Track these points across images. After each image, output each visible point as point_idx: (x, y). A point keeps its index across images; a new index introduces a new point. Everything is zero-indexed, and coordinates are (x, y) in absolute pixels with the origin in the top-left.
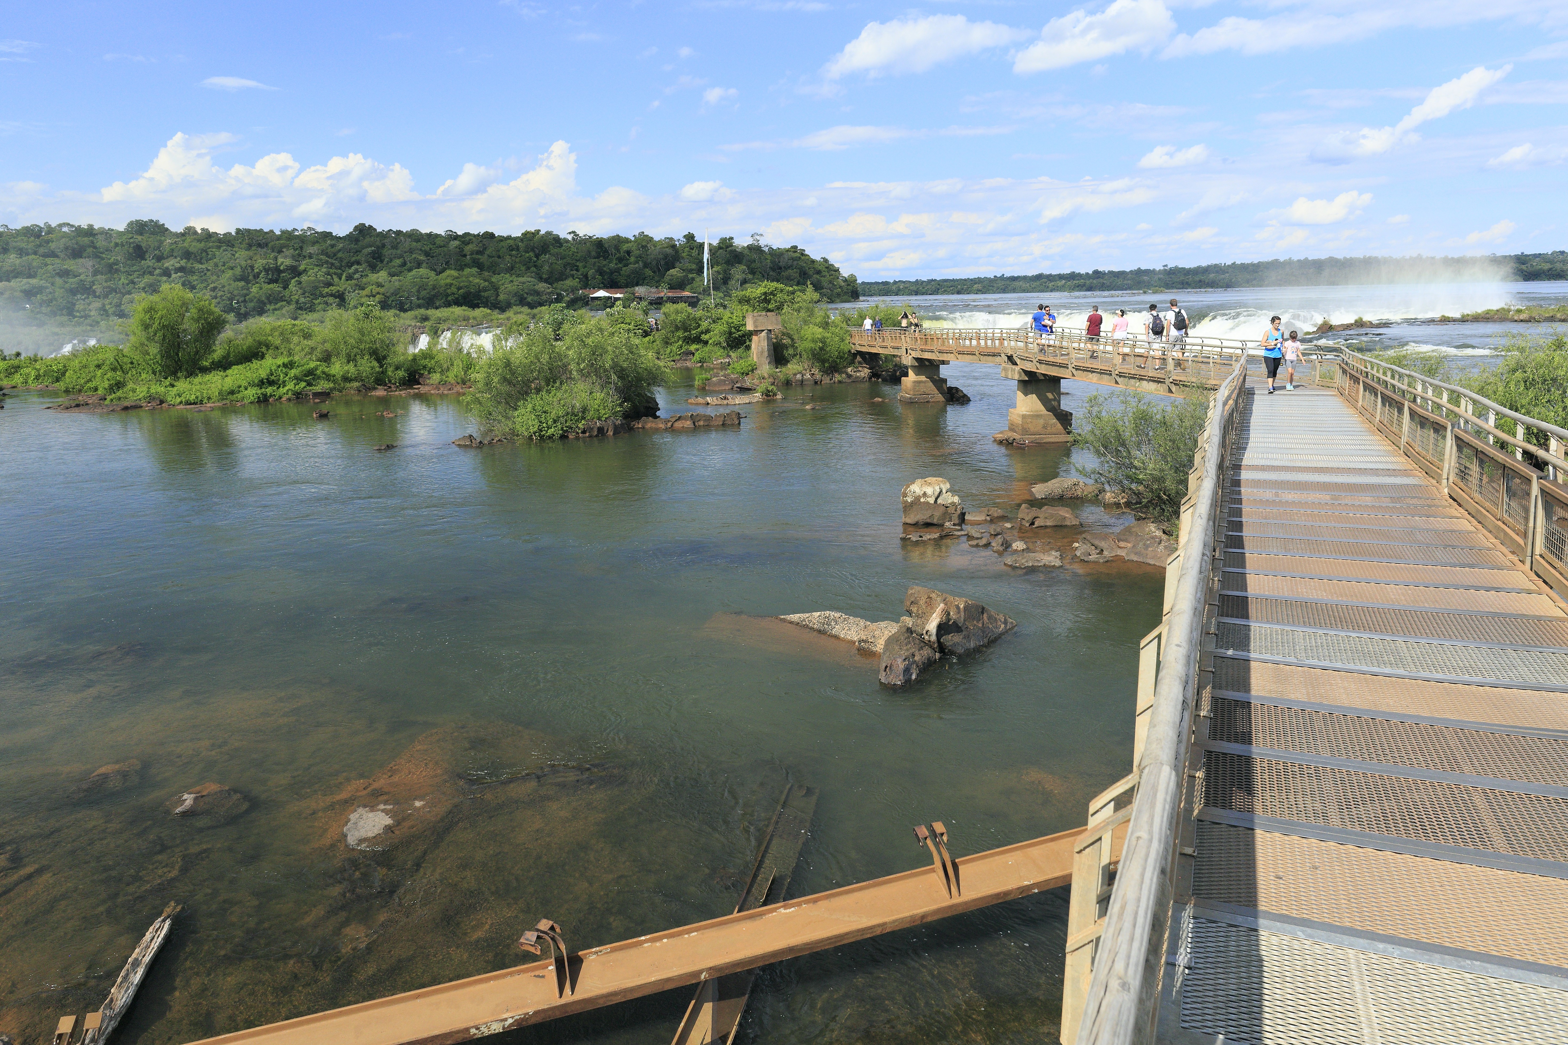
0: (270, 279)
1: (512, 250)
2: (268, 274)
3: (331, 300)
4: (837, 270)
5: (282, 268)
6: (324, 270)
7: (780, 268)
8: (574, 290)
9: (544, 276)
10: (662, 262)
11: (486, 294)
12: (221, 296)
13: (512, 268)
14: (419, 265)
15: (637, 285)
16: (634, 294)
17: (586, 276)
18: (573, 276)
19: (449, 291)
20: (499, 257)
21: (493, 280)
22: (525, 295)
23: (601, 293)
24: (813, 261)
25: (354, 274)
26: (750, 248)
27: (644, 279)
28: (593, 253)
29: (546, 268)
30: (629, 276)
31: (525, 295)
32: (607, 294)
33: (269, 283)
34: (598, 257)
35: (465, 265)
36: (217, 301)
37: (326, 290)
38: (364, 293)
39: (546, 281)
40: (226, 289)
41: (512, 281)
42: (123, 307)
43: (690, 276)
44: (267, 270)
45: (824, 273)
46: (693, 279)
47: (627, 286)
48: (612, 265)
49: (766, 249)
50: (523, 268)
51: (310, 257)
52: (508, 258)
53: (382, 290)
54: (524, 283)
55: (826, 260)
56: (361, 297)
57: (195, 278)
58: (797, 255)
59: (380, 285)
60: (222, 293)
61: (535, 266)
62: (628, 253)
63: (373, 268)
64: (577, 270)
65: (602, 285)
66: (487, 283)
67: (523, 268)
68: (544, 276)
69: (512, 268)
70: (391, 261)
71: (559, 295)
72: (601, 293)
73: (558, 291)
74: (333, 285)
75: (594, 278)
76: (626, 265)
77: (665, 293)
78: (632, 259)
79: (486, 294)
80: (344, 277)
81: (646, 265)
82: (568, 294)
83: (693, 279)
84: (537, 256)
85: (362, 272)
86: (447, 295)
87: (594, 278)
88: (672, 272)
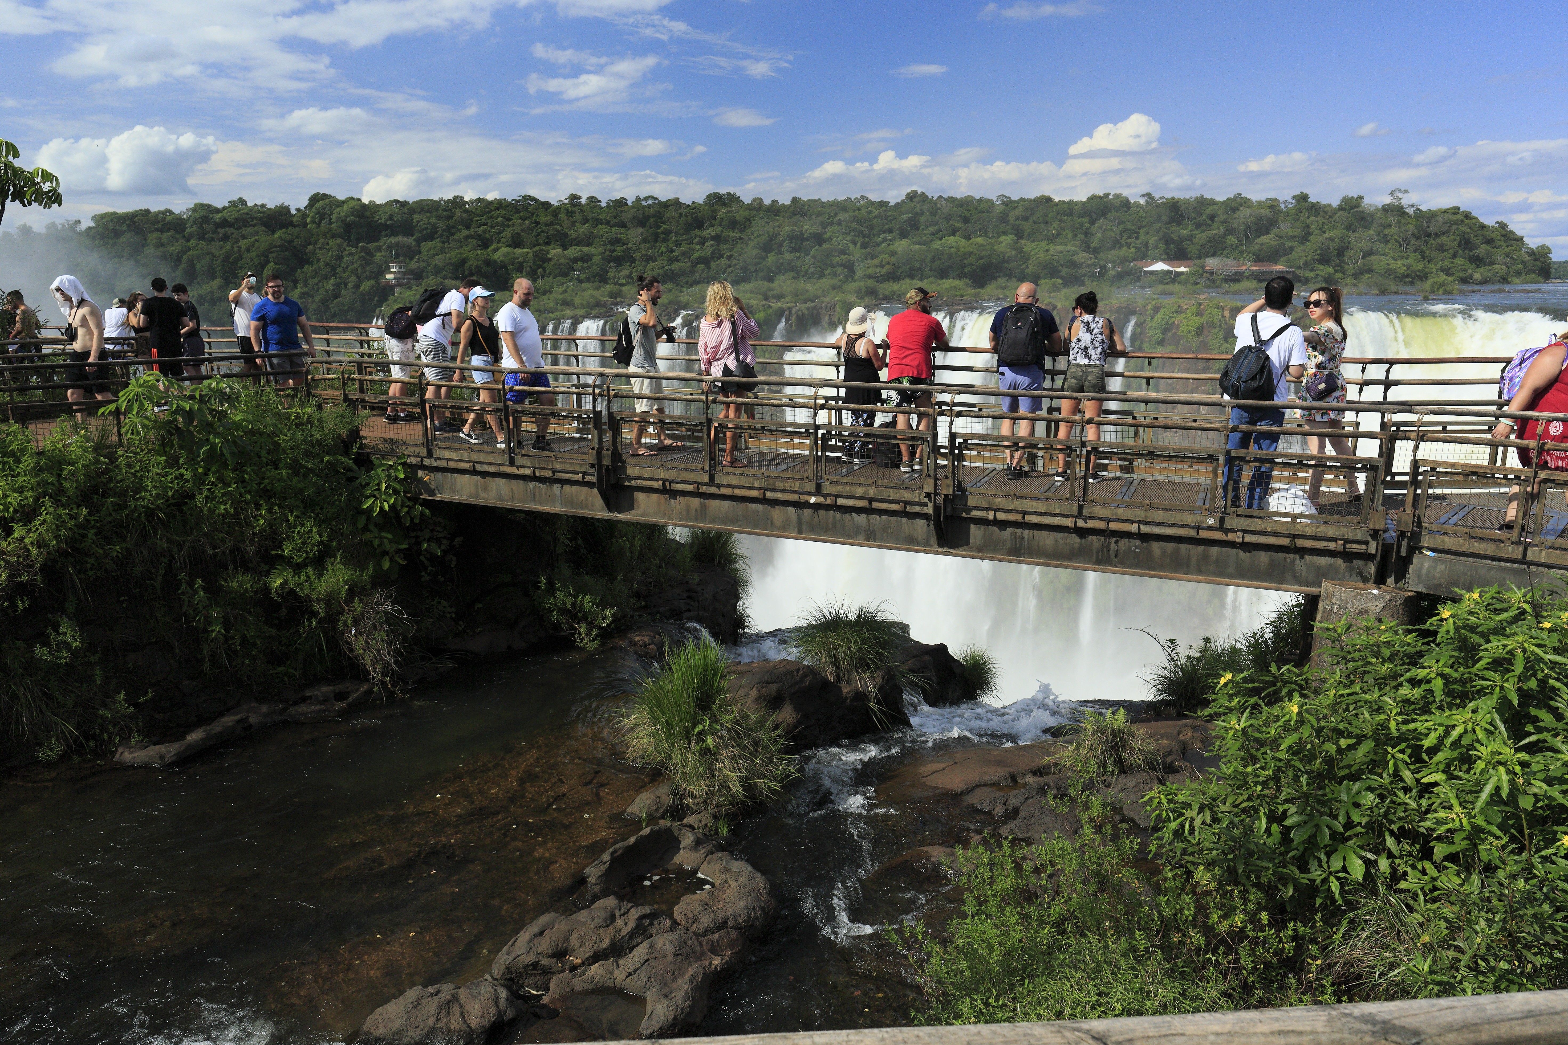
4: (1520, 239)
7: (1429, 235)
10: (1253, 227)
17: (1146, 246)
24: (1483, 227)
26: (1387, 209)
28: (1165, 218)
30: (1203, 245)
43: (1289, 244)
44: (791, 238)
45: (1498, 243)
46: (1292, 249)
49: (1411, 211)
51: (840, 223)
52: (1056, 224)
55: (1503, 226)
58: (1460, 217)
81: (1230, 231)
83: (1292, 249)
84: (1093, 222)
88: (1264, 239)
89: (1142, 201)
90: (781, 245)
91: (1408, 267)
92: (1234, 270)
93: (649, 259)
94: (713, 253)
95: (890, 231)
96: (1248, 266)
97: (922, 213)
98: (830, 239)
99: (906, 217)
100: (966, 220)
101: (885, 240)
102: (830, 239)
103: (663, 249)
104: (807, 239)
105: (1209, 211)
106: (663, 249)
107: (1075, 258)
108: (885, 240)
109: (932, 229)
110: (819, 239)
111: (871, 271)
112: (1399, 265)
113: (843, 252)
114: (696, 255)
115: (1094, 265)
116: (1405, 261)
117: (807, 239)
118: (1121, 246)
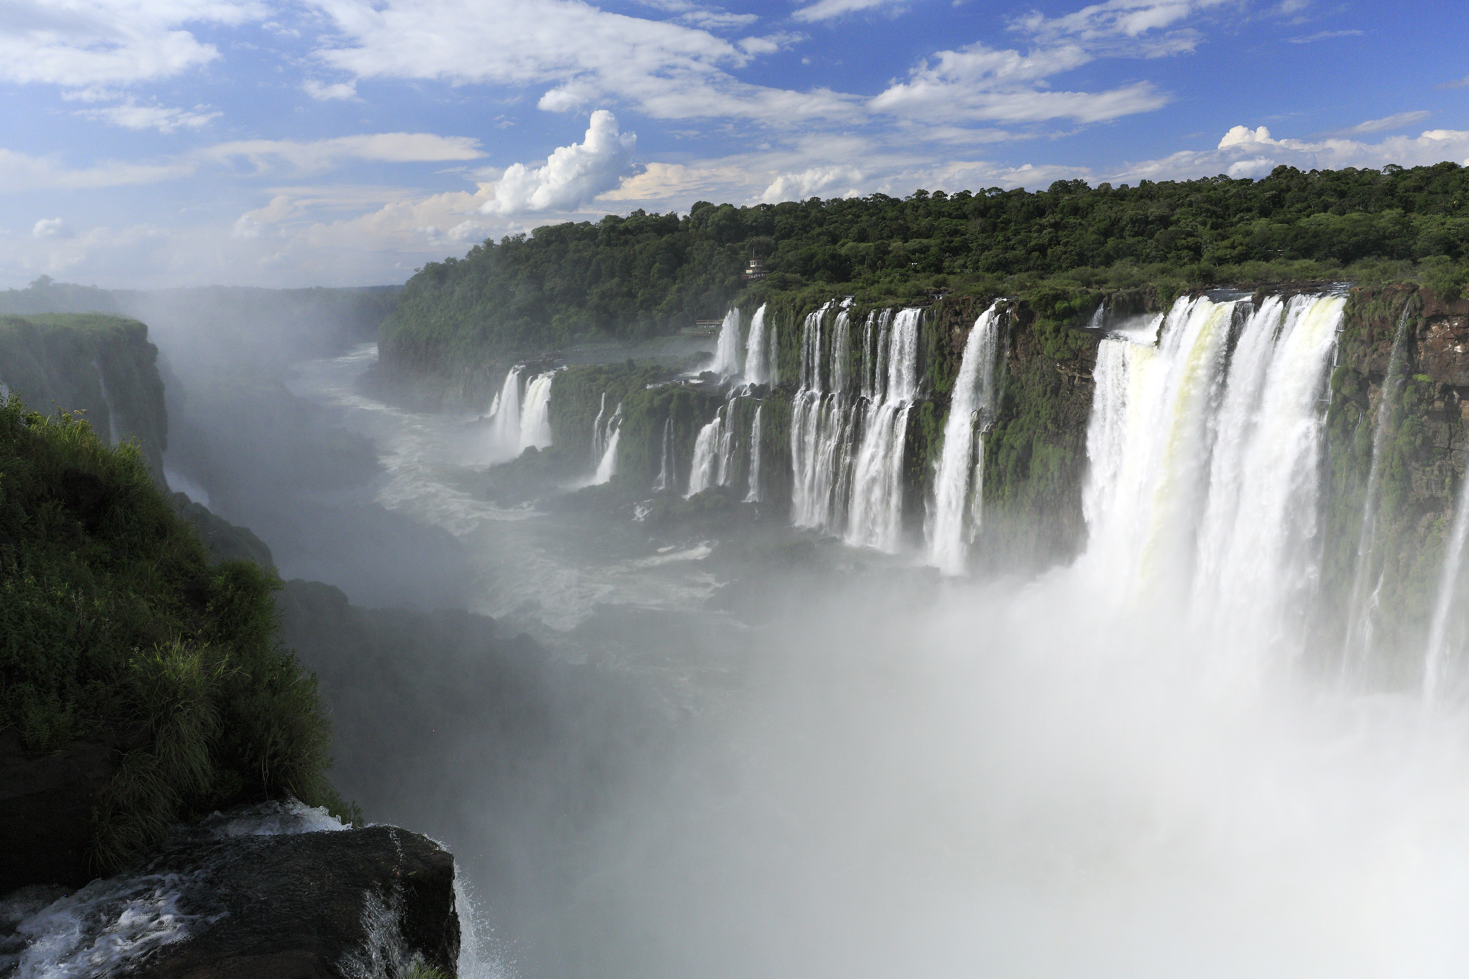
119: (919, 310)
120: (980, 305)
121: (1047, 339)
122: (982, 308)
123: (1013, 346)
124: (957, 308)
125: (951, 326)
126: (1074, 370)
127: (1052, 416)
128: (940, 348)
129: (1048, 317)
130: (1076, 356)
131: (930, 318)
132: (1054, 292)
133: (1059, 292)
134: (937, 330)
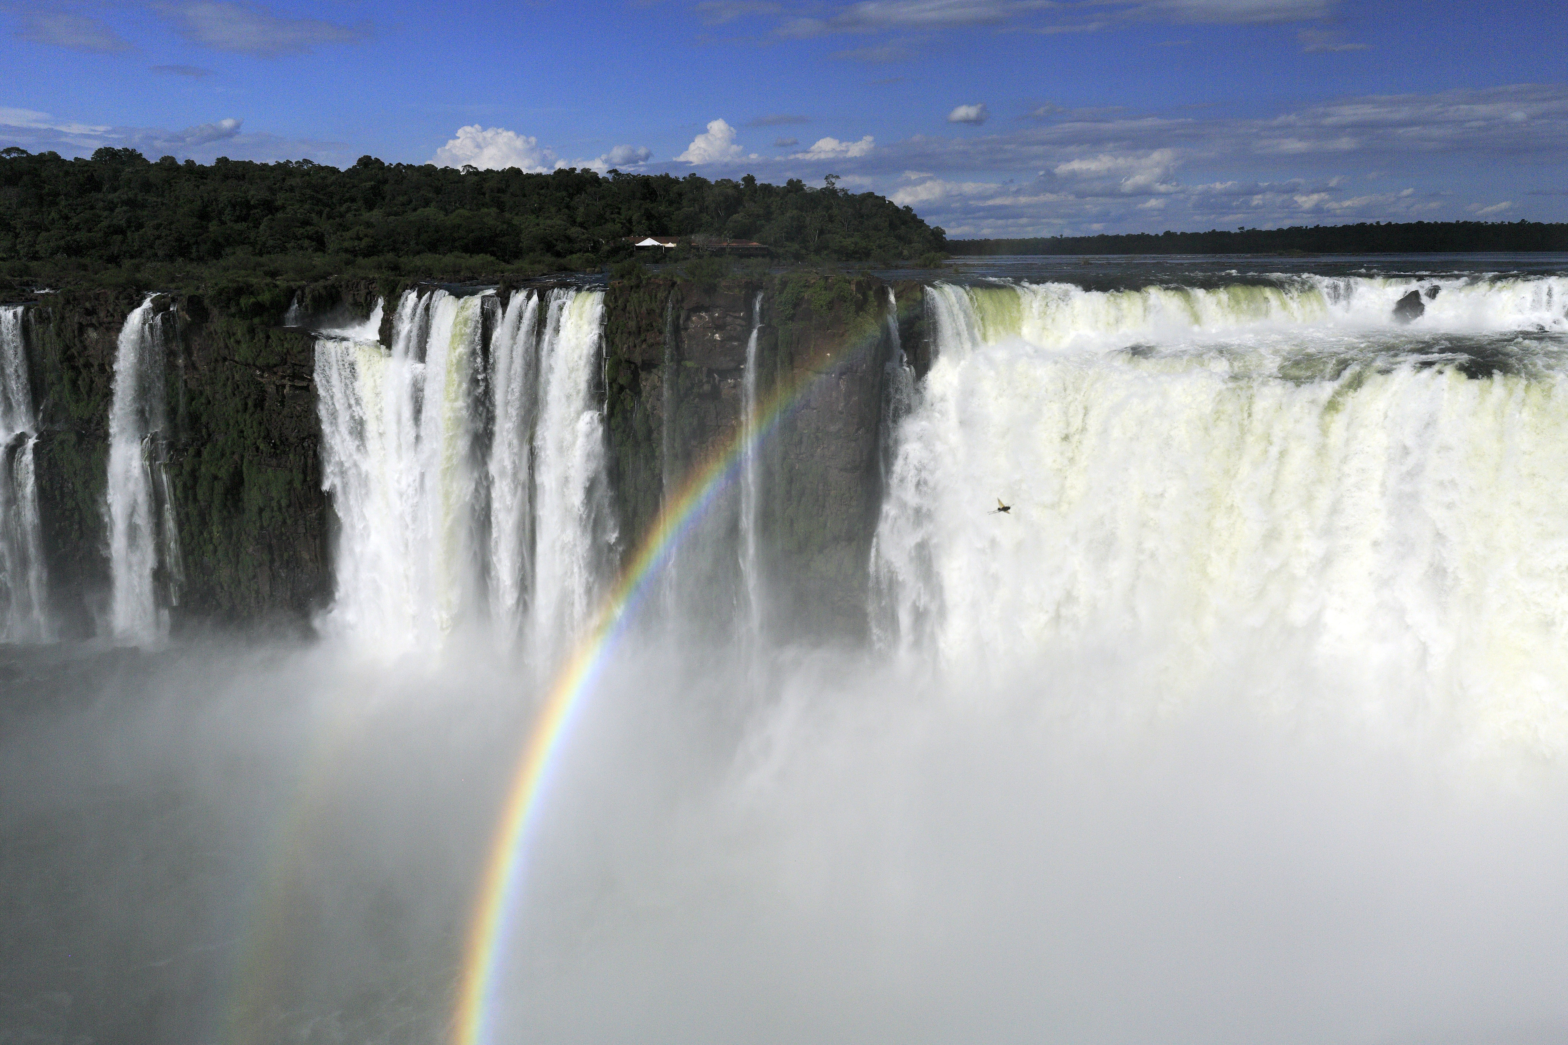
0: (238, 217)
1: (542, 188)
2: (235, 210)
3: (306, 243)
5: (252, 203)
6: (307, 206)
8: (616, 236)
9: (579, 220)
11: (504, 239)
12: (166, 235)
13: (540, 209)
14: (427, 204)
15: (692, 232)
16: (689, 243)
17: (630, 221)
18: (614, 220)
19: (456, 235)
20: (525, 196)
21: (515, 222)
22: (554, 242)
23: (649, 242)
25: (347, 212)
27: (700, 226)
29: (582, 209)
31: (554, 242)
32: (656, 243)
33: (236, 221)
34: (644, 198)
35: (483, 205)
36: (161, 241)
37: (301, 230)
38: (347, 235)
39: (581, 225)
40: (173, 227)
41: (538, 225)
42: (38, 247)
47: (679, 233)
48: (662, 208)
50: (553, 210)
53: (371, 231)
54: (552, 227)
56: (344, 240)
57: (145, 213)
59: (369, 225)
60: (168, 232)
61: (568, 207)
62: (680, 195)
63: (370, 207)
64: (619, 213)
65: (649, 232)
66: (505, 226)
67: (553, 210)
68: (579, 220)
69: (540, 209)
70: (394, 197)
71: (596, 242)
72: (649, 242)
73: (596, 238)
74: (311, 225)
75: (639, 223)
76: (679, 209)
77: (728, 243)
78: (685, 202)
79: (504, 239)
80: (324, 215)
82: (608, 242)
84: (571, 196)
85: (356, 210)
86: (454, 240)
87: (639, 223)
89: (610, 177)
90: (221, 213)
91: (856, 244)
92: (718, 246)
93: (37, 228)
94: (129, 222)
95: (353, 200)
96: (728, 243)
97: (385, 182)
98: (283, 207)
99: (369, 184)
100: (438, 191)
101: (349, 210)
102: (283, 207)
103: (54, 215)
104: (255, 207)
105: (675, 189)
106: (54, 215)
107: (568, 232)
108: (349, 210)
109: (402, 199)
110: (270, 207)
111: (346, 244)
112: (848, 242)
113: (306, 223)
114: (105, 223)
115: (588, 239)
116: (853, 240)
117: (255, 207)
118: (607, 221)
119: (20, 310)
120: (125, 301)
121: (238, 342)
122: (129, 304)
123: (188, 352)
124: (88, 305)
125: (82, 329)
126: (283, 377)
127: (262, 434)
128: (68, 359)
129: (233, 316)
130: (284, 362)
131: (42, 319)
132: (235, 285)
133: (241, 284)
134: (58, 335)
